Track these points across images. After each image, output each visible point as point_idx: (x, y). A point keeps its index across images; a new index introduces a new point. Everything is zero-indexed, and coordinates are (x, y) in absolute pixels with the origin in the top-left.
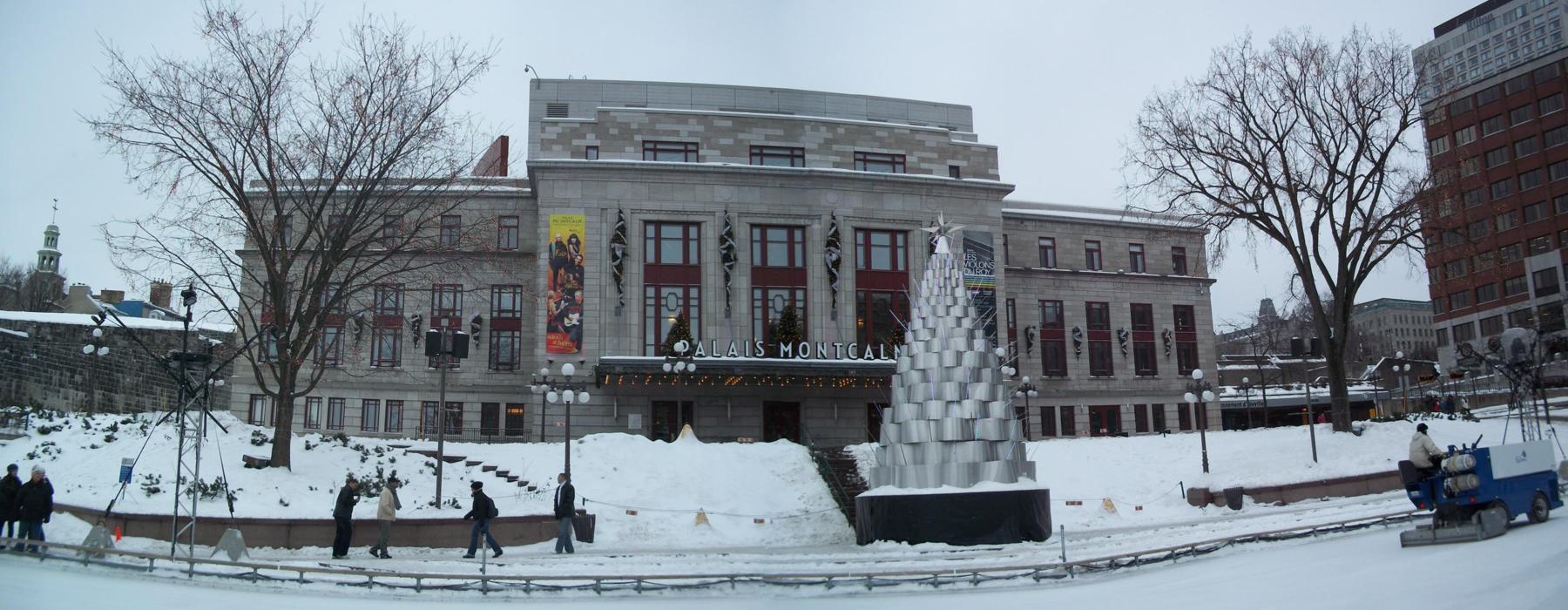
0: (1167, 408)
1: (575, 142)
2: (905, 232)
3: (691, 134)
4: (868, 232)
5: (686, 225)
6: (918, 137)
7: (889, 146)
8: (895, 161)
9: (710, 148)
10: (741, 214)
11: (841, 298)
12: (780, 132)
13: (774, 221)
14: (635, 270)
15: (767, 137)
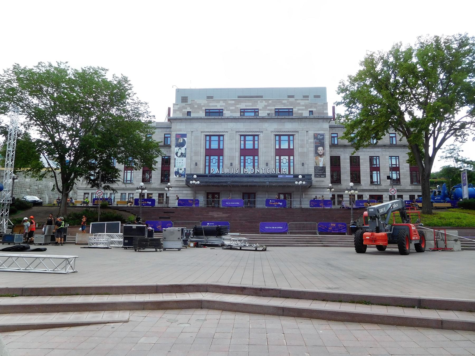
1: (184, 110)
2: (293, 135)
3: (221, 106)
4: (280, 136)
5: (219, 136)
6: (298, 102)
7: (287, 106)
9: (227, 110)
12: (250, 104)
15: (246, 106)
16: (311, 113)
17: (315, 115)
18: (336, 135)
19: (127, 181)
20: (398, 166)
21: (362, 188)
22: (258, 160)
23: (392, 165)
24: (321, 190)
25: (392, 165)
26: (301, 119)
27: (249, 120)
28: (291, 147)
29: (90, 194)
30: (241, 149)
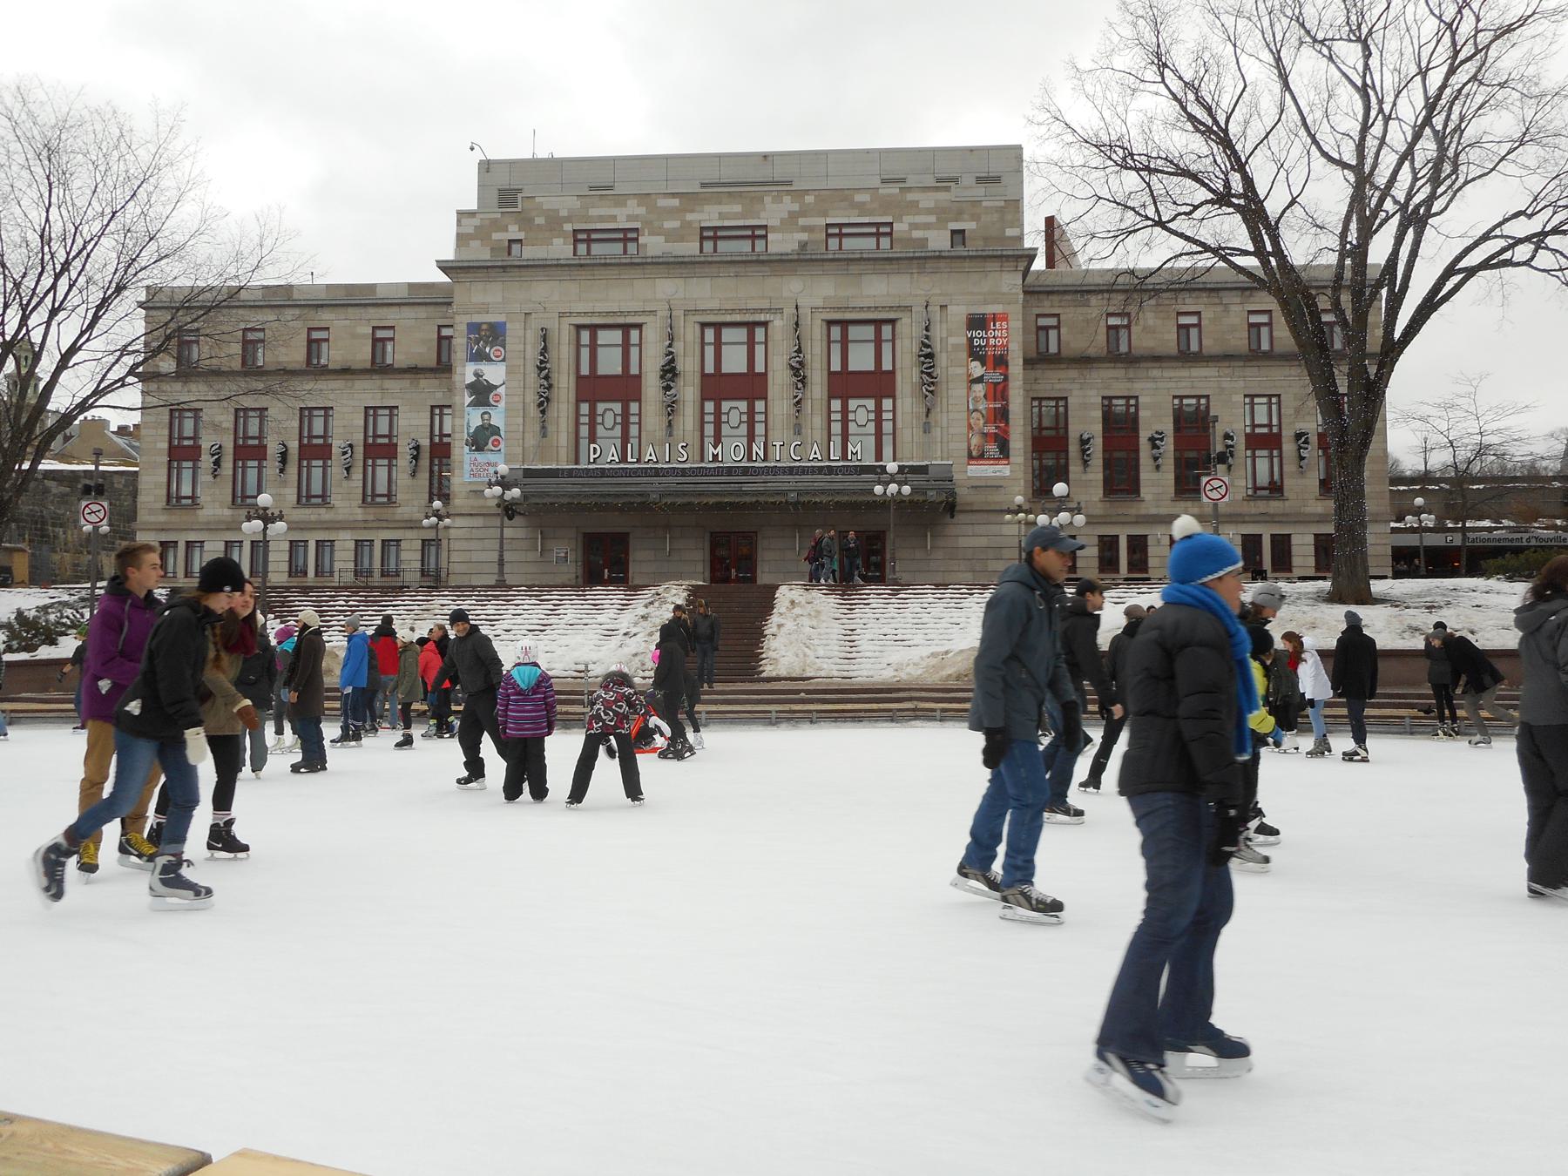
0: (1295, 540)
1: (496, 236)
2: (892, 322)
3: (630, 218)
4: (844, 324)
5: (626, 328)
6: (910, 197)
8: (881, 231)
10: (687, 312)
11: (807, 406)
12: (737, 208)
13: (728, 318)
14: (565, 384)
15: (722, 216)
16: (958, 238)
17: (973, 247)
18: (1053, 321)
19: (374, 495)
20: (1275, 430)
21: (1143, 512)
22: (766, 413)
23: (1254, 426)
24: (993, 517)
25: (1254, 426)
26: (921, 260)
27: (733, 270)
28: (887, 366)
29: (182, 547)
30: (704, 376)
